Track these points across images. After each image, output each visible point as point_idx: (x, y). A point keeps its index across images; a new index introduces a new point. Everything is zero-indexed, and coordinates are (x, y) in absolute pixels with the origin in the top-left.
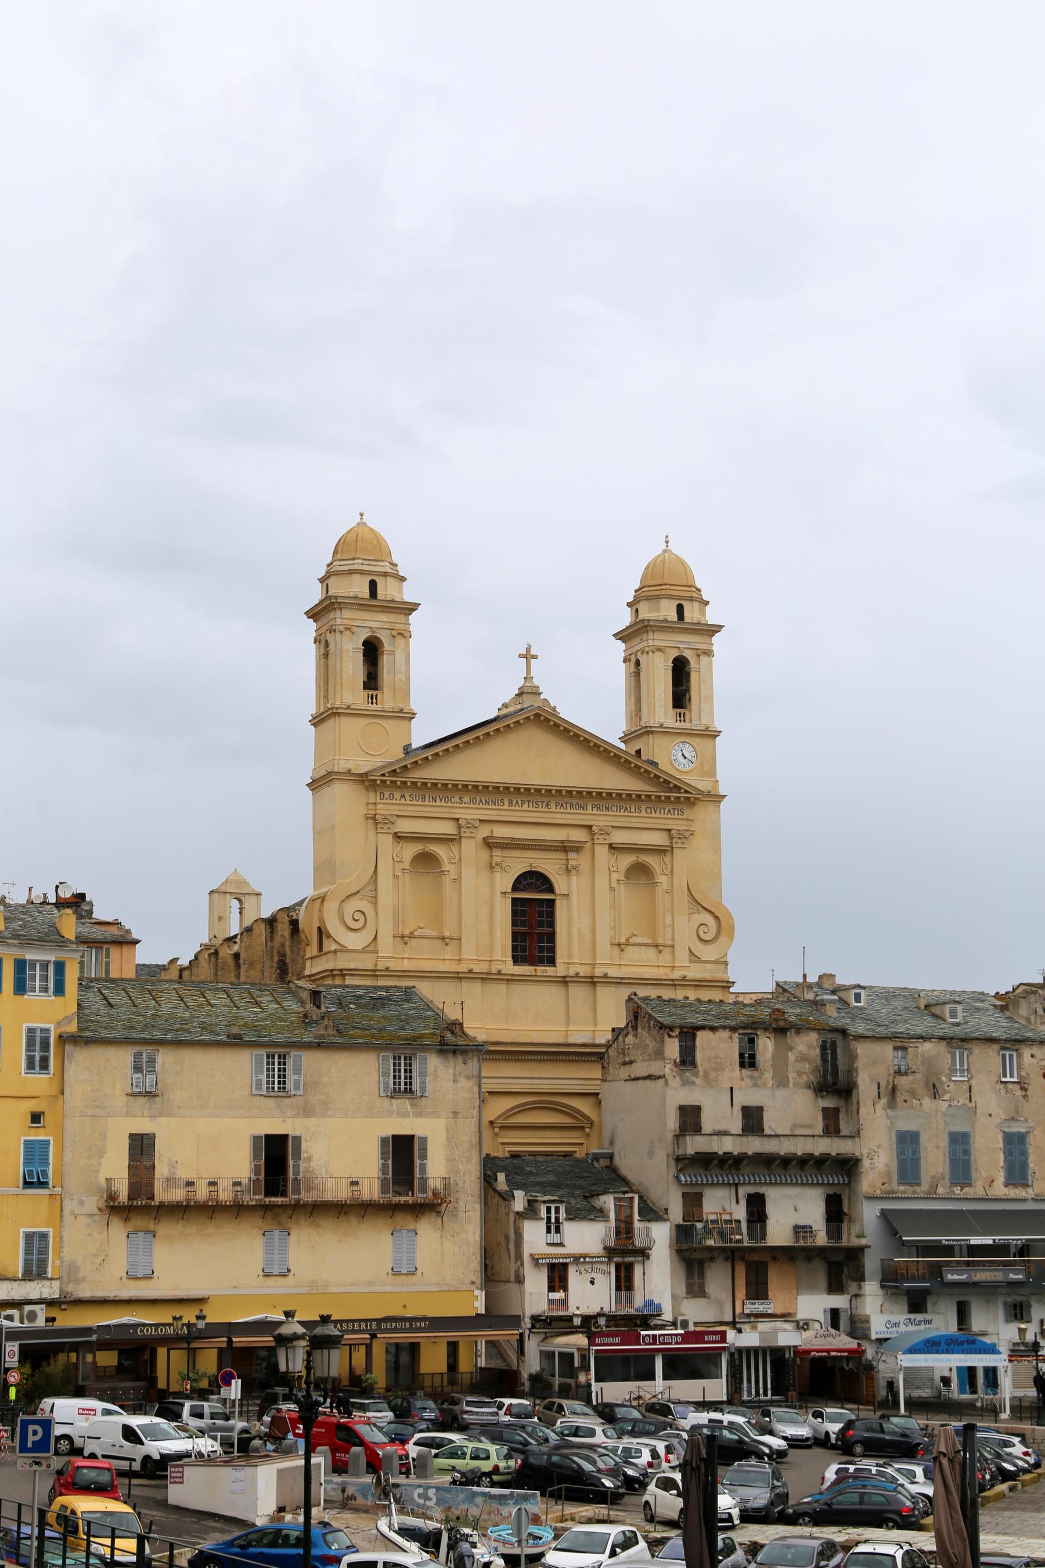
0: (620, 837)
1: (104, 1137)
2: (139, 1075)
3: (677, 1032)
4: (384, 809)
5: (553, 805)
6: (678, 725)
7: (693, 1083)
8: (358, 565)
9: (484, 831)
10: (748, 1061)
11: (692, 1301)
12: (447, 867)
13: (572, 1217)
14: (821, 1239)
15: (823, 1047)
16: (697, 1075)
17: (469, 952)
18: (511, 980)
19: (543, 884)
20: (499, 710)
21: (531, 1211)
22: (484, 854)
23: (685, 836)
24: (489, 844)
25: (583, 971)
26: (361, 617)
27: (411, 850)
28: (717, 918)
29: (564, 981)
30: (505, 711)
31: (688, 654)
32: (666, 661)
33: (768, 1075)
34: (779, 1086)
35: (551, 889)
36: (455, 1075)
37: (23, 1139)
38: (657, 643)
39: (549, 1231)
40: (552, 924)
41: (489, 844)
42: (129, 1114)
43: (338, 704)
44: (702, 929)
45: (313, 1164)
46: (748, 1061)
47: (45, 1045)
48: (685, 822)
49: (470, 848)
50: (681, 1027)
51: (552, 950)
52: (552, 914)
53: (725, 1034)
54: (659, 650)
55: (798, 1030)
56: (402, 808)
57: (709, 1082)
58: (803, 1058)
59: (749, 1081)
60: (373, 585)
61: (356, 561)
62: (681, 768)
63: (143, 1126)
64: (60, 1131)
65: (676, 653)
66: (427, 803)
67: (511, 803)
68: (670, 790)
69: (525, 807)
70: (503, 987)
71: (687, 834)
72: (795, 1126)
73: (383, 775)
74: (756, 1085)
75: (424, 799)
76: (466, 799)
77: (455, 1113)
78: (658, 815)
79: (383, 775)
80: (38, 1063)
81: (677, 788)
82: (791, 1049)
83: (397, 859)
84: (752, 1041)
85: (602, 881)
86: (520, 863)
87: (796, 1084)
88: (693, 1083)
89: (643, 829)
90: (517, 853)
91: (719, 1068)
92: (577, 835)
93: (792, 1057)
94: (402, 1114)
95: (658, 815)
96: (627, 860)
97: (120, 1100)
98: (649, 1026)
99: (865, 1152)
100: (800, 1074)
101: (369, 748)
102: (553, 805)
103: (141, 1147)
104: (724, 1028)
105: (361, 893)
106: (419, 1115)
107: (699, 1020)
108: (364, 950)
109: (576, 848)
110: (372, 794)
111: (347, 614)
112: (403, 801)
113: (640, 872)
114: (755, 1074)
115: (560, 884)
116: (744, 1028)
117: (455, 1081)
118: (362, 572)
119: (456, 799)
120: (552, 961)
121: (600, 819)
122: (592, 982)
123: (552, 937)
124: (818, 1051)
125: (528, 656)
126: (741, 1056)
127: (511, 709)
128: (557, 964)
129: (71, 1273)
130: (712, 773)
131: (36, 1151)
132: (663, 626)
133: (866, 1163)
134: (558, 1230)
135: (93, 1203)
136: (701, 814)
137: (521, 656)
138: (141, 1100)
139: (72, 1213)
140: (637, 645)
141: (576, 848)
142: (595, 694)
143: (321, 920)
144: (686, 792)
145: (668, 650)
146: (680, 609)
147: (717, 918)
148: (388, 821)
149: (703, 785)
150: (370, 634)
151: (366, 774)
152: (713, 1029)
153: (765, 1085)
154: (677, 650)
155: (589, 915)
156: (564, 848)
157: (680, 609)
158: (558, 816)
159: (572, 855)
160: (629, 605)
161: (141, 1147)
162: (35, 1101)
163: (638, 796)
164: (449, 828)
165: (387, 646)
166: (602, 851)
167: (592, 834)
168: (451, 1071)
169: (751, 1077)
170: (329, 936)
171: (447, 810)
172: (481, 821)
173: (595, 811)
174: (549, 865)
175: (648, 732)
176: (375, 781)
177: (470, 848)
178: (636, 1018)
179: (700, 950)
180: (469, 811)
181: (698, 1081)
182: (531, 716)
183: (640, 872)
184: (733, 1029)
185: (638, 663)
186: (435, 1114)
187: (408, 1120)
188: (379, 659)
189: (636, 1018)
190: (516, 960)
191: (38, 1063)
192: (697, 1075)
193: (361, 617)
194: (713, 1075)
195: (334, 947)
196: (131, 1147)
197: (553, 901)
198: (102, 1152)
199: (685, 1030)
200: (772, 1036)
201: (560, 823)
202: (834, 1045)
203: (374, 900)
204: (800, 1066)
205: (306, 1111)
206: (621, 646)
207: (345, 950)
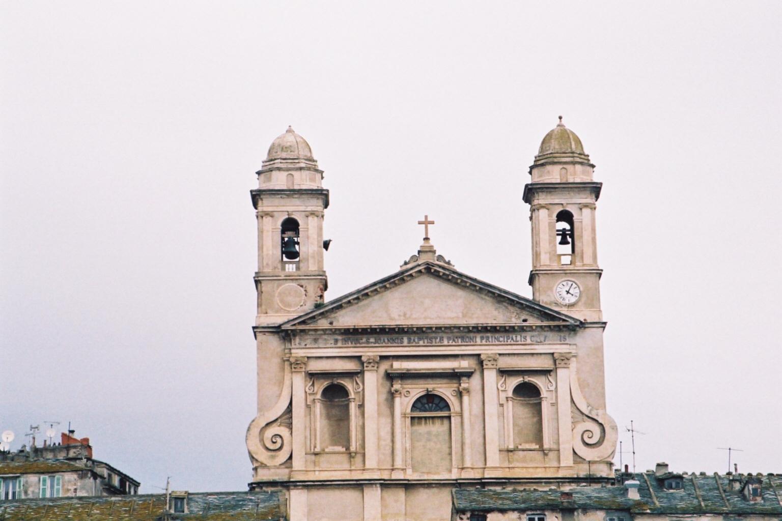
3: (469, 515)
4: (299, 352)
12: (352, 395)
17: (371, 463)
19: (442, 405)
20: (401, 267)
23: (565, 359)
26: (289, 202)
30: (405, 267)
32: (550, 216)
41: (390, 377)
48: (568, 346)
49: (372, 381)
50: (473, 511)
55: (585, 509)
65: (560, 209)
73: (294, 325)
76: (372, 340)
92: (464, 365)
96: (515, 381)
101: (292, 305)
104: (514, 510)
105: (279, 420)
116: (531, 510)
121: (486, 348)
125: (426, 222)
127: (409, 266)
136: (582, 342)
137: (420, 223)
141: (469, 375)
142: (502, 250)
144: (564, 320)
145: (550, 207)
147: (601, 424)
149: (579, 314)
150: (287, 217)
151: (279, 327)
152: (503, 511)
154: (561, 206)
156: (455, 376)
166: (491, 376)
167: (481, 363)
174: (445, 390)
177: (372, 381)
179: (583, 451)
180: (369, 352)
182: (434, 270)
184: (522, 511)
193: (289, 202)
200: (559, 515)
203: (290, 426)
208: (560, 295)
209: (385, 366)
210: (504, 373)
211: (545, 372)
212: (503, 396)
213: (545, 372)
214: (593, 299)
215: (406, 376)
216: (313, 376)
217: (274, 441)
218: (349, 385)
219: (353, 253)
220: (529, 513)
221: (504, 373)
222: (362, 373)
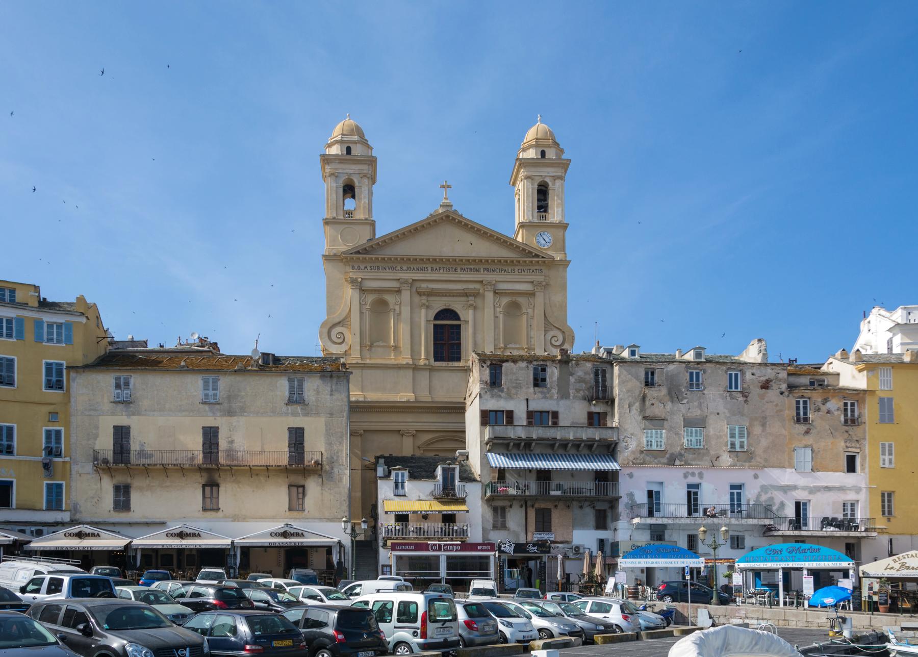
1: (97, 427)
2: (119, 391)
3: (489, 363)
7: (500, 396)
10: (539, 381)
11: (497, 532)
13: (413, 477)
14: (593, 494)
15: (596, 374)
16: (502, 391)
21: (387, 476)
22: (417, 299)
23: (546, 286)
33: (554, 391)
34: (562, 398)
35: (458, 318)
36: (332, 391)
37: (44, 428)
39: (397, 487)
40: (459, 339)
42: (113, 414)
45: (235, 445)
46: (539, 381)
47: (60, 373)
49: (406, 295)
50: (491, 361)
51: (460, 353)
52: (459, 334)
53: (523, 364)
57: (510, 397)
58: (581, 380)
59: (540, 395)
63: (123, 421)
64: (67, 425)
68: (533, 257)
72: (573, 423)
74: (545, 398)
77: (331, 414)
80: (55, 383)
82: (572, 374)
84: (544, 370)
85: (488, 312)
86: (439, 304)
87: (575, 397)
88: (500, 396)
89: (517, 283)
90: (438, 298)
91: (518, 386)
93: (572, 379)
94: (295, 414)
97: (107, 406)
99: (622, 437)
100: (578, 391)
103: (122, 434)
106: (307, 415)
109: (476, 294)
114: (545, 390)
115: (467, 315)
116: (536, 361)
117: (331, 395)
124: (592, 376)
126: (535, 379)
129: (75, 509)
130: (563, 249)
131: (54, 437)
133: (622, 445)
134: (403, 487)
135: (89, 467)
138: (121, 406)
139: (77, 472)
141: (476, 294)
153: (551, 398)
155: (481, 332)
156: (466, 294)
159: (470, 298)
161: (122, 434)
162: (53, 406)
163: (512, 261)
164: (395, 285)
165: (357, 184)
168: (329, 389)
169: (542, 392)
174: (457, 305)
181: (503, 395)
186: (318, 414)
187: (298, 418)
190: (436, 360)
191: (55, 383)
192: (502, 391)
194: (513, 391)
196: (115, 434)
197: (460, 325)
198: (96, 437)
201: (466, 279)
202: (604, 372)
204: (578, 386)
205: (230, 413)
208: (542, 242)
214: (561, 246)
215: (431, 293)
218: (389, 298)
219: (394, 206)
220: (535, 363)
222: (399, 291)
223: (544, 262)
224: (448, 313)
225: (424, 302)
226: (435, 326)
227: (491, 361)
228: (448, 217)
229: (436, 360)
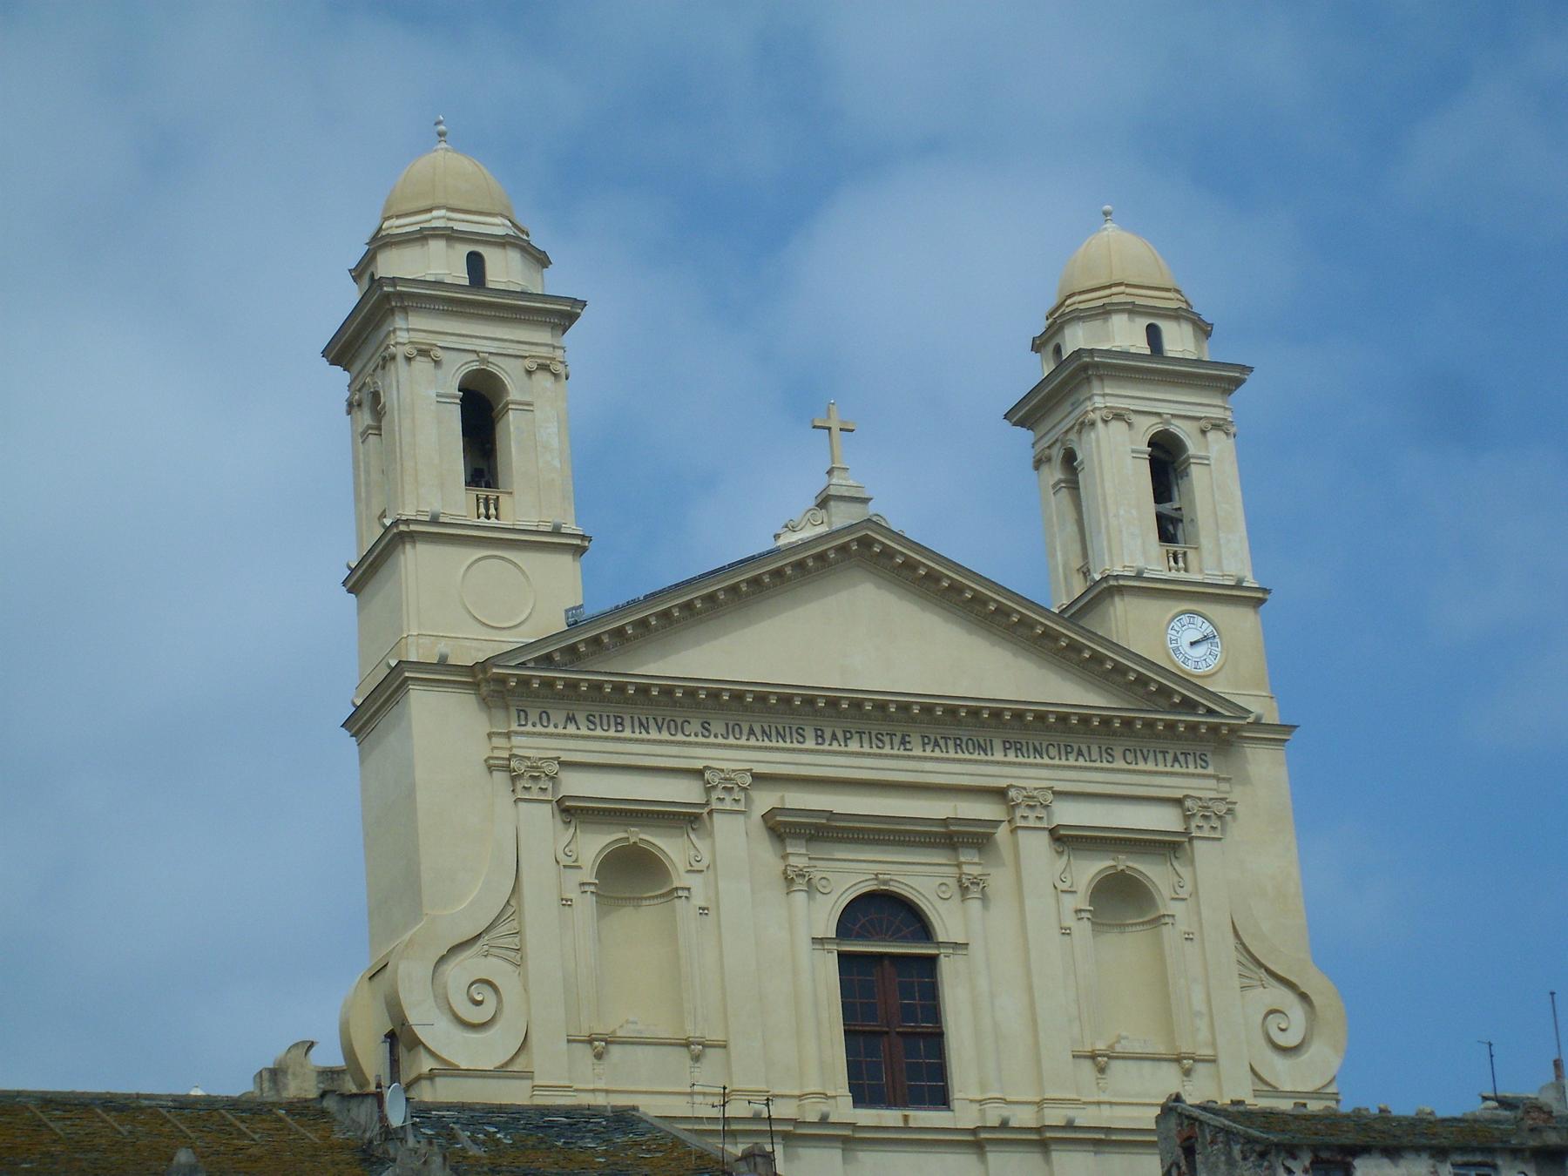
0: (1070, 815)
5: (915, 739)
6: (1173, 575)
8: (438, 219)
9: (765, 800)
12: (680, 879)
18: (850, 1140)
22: (766, 850)
23: (1219, 815)
24: (781, 828)
25: (1024, 1117)
27: (593, 844)
28: (1304, 997)
29: (977, 1142)
31: (1182, 429)
38: (1111, 402)
40: (933, 1011)
41: (781, 828)
43: (409, 512)
44: (1273, 1022)
48: (1212, 783)
49: (736, 839)
50: (1315, 1149)
54: (1118, 416)
56: (572, 744)
60: (475, 263)
61: (435, 213)
62: (1189, 667)
66: (627, 734)
67: (820, 736)
68: (1174, 708)
69: (854, 746)
70: (834, 1155)
71: (1222, 808)
73: (522, 665)
75: (620, 723)
78: (1150, 766)
79: (522, 665)
81: (1189, 705)
83: (565, 861)
86: (851, 874)
89: (1127, 796)
90: (841, 852)
95: (1150, 766)
96: (1090, 869)
98: (1231, 1163)
102: (915, 739)
104: (1418, 1150)
107: (1349, 1139)
108: (502, 1072)
110: (499, 714)
111: (418, 321)
112: (571, 729)
113: (1119, 899)
115: (947, 920)
116: (1463, 1150)
118: (451, 236)
119: (695, 726)
120: (940, 1098)
121: (1027, 774)
122: (1042, 1141)
123: (937, 1039)
128: (956, 1105)
132: (1120, 368)
140: (1060, 422)
143: (395, 1008)
144: (1210, 712)
145: (1134, 418)
146: (1153, 334)
147: (1304, 997)
148: (536, 773)
151: (484, 665)
157: (1153, 334)
158: (929, 766)
159: (966, 856)
160: (1038, 345)
166: (1036, 846)
170: (415, 1043)
171: (674, 750)
172: (759, 778)
173: (1011, 757)
174: (920, 879)
175: (1104, 591)
176: (502, 680)
177: (736, 839)
178: (1189, 1151)
183: (1119, 899)
184: (1440, 1153)
185: (1070, 458)
188: (500, 428)
189: (1189, 1151)
190: (862, 1096)
195: (427, 1064)
197: (932, 960)
199: (1325, 1155)
203: (517, 957)
206: (1025, 435)
207: (453, 1071)
209: (765, 800)
210: (1066, 840)
211: (1167, 847)
212: (1070, 903)
213: (1167, 847)
216: (573, 812)
217: (479, 998)
220: (1459, 1159)
221: (1066, 840)
223: (1214, 729)
224: (880, 910)
225: (799, 862)
226: (841, 955)
227: (1315, 1149)
228: (865, 542)
229: (862, 1096)
